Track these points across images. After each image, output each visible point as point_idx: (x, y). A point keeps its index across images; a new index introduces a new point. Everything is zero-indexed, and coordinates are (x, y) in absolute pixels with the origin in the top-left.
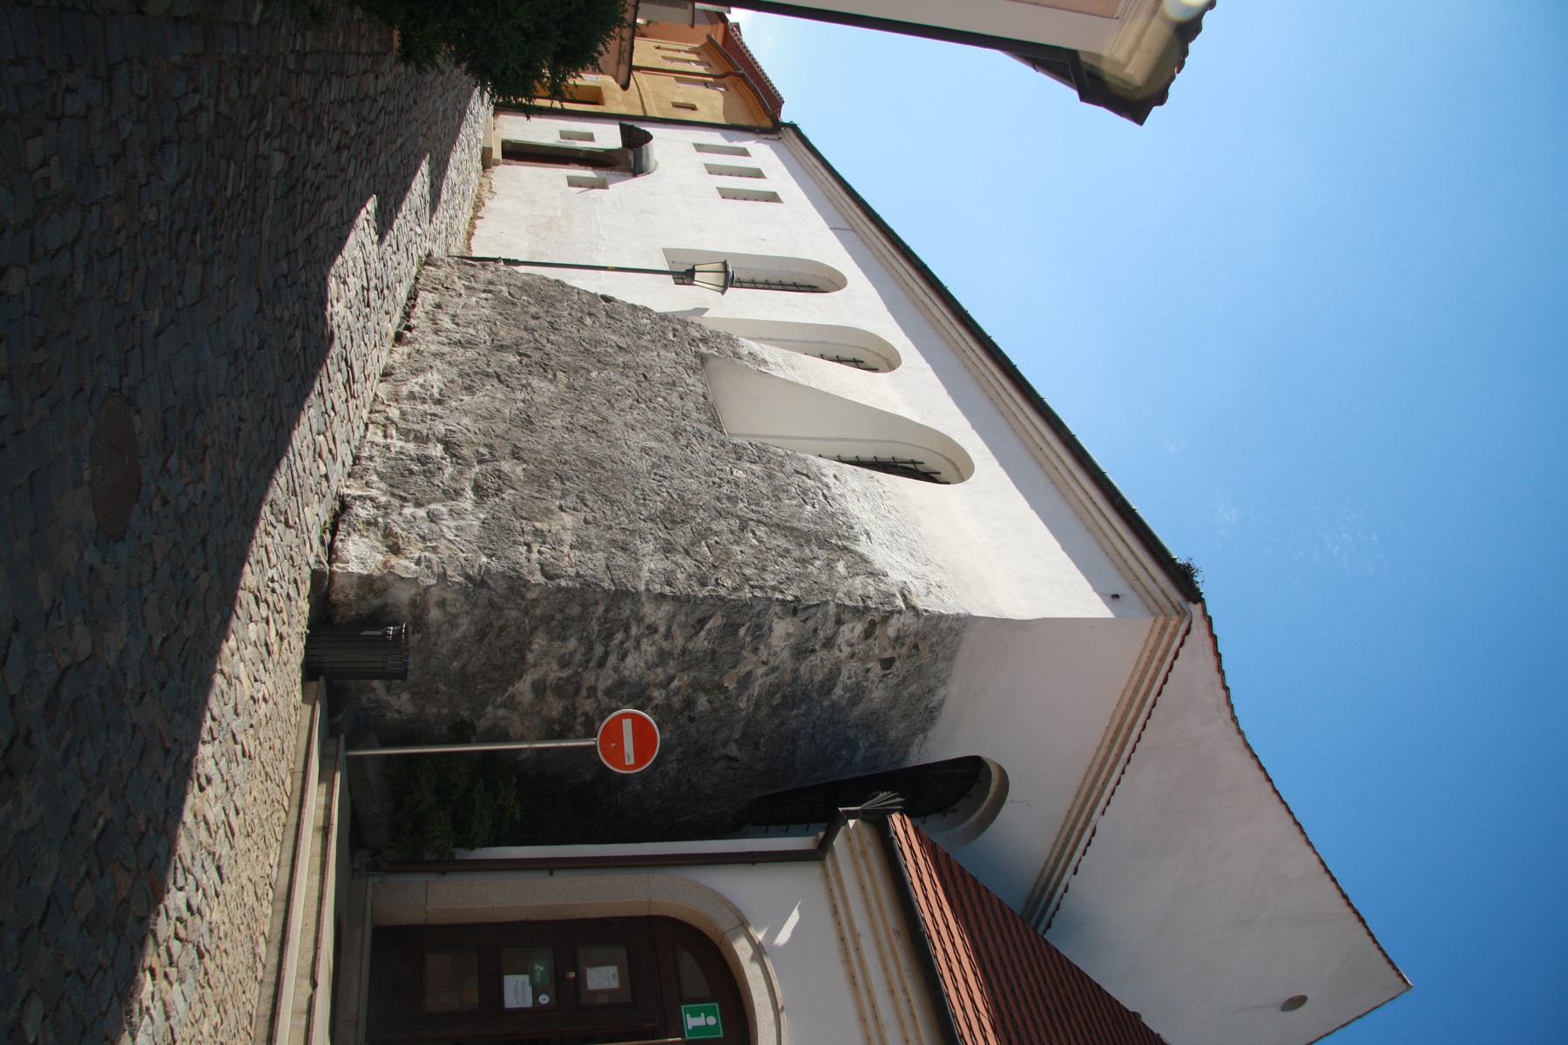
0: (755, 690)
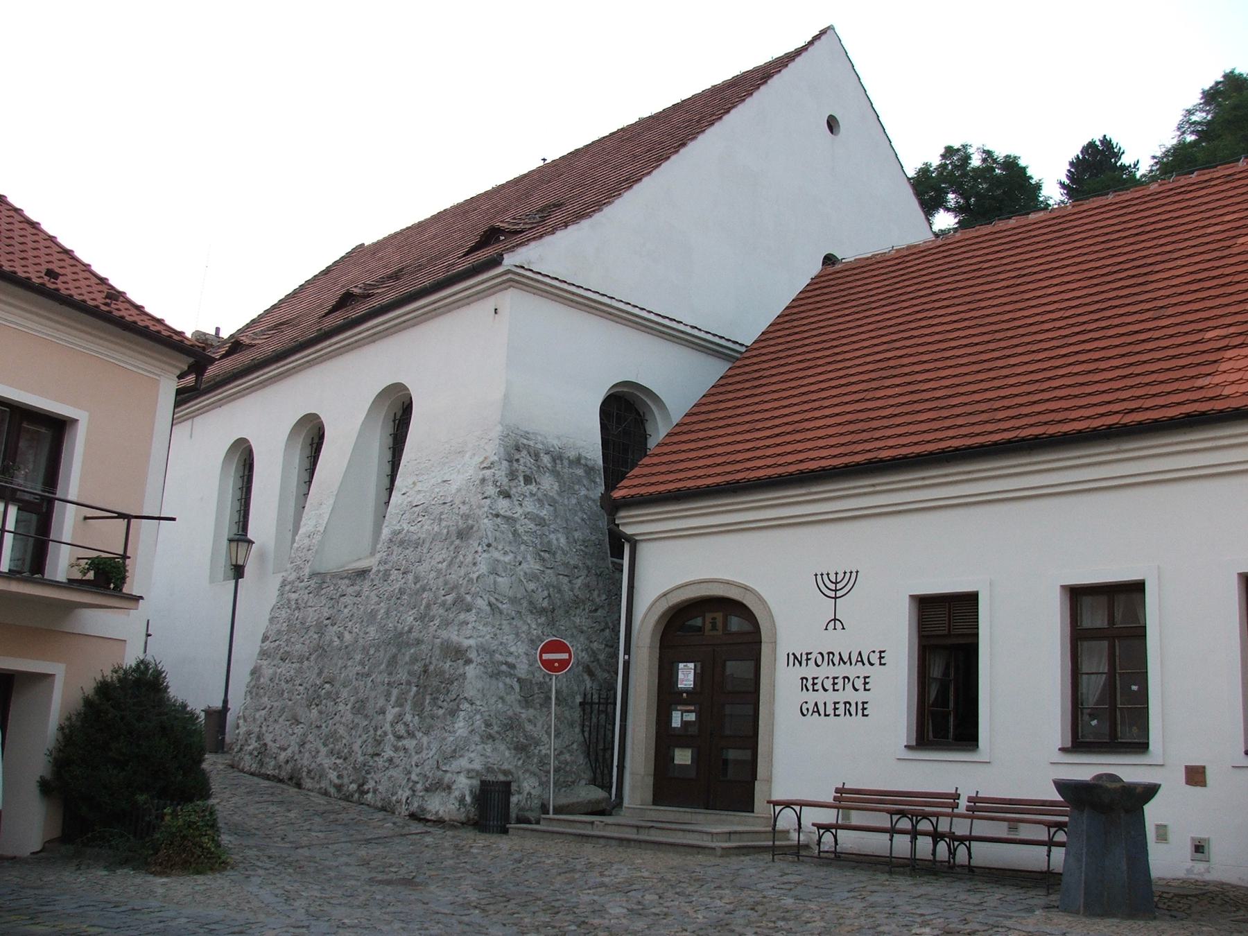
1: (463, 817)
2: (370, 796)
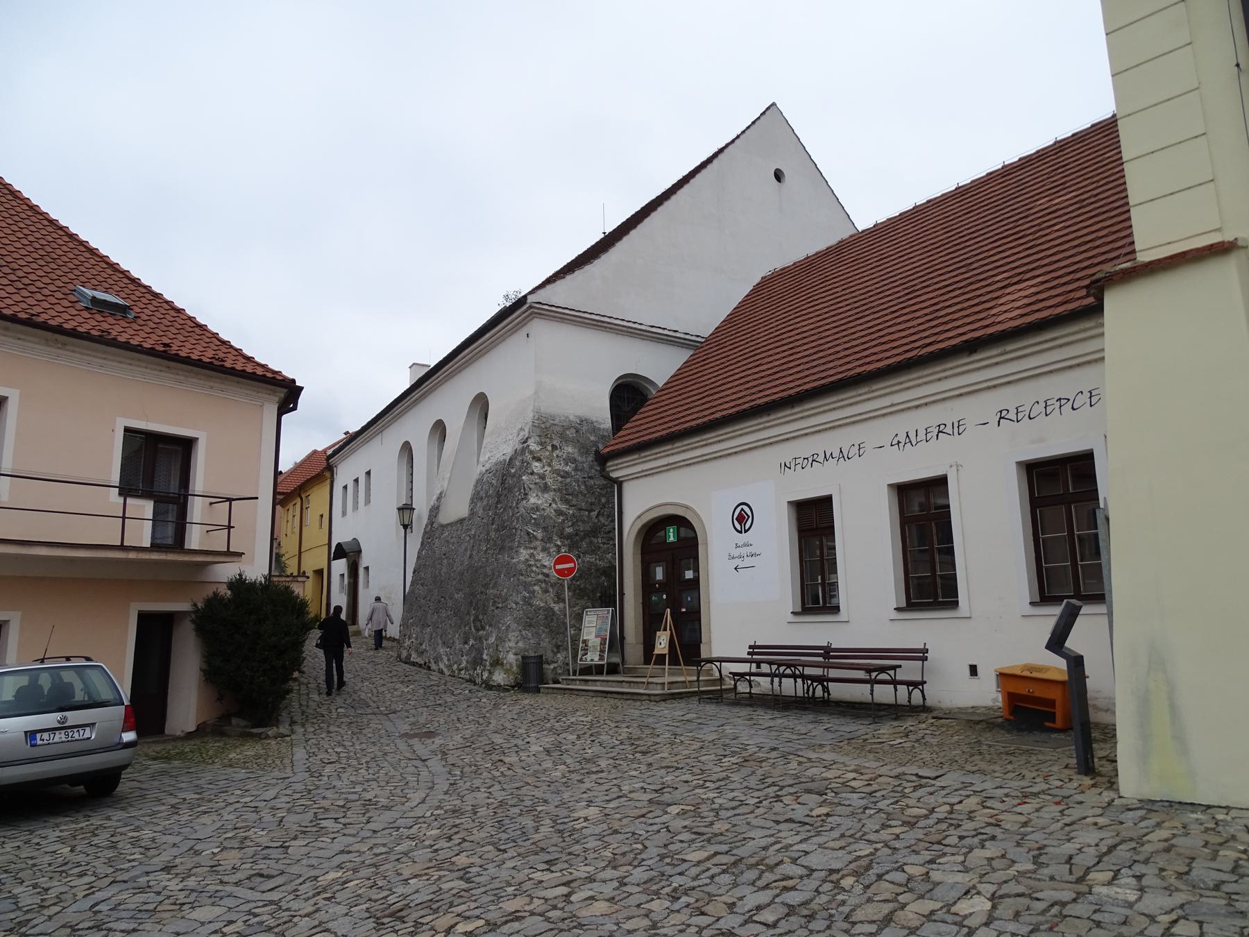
0: (563, 507)
1: (512, 682)
2: (463, 672)
